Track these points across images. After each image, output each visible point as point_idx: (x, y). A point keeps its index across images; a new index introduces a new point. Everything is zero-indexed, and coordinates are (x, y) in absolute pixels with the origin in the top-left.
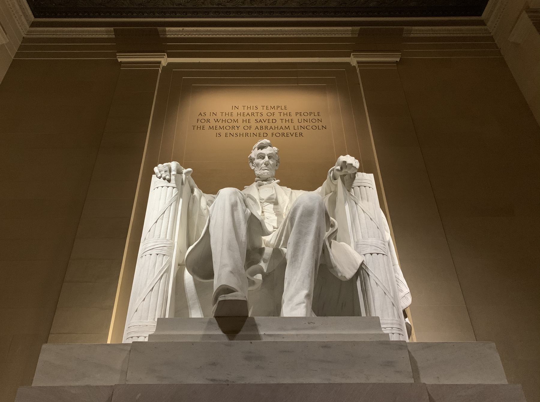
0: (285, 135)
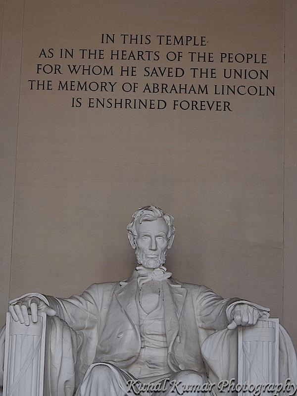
0: (199, 106)
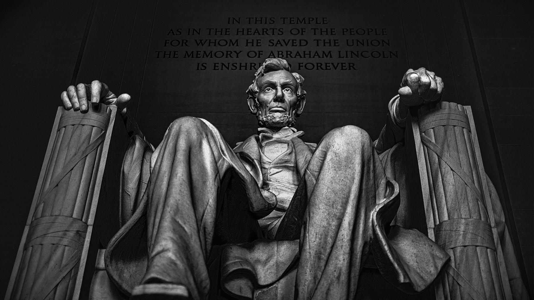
0: (324, 66)
